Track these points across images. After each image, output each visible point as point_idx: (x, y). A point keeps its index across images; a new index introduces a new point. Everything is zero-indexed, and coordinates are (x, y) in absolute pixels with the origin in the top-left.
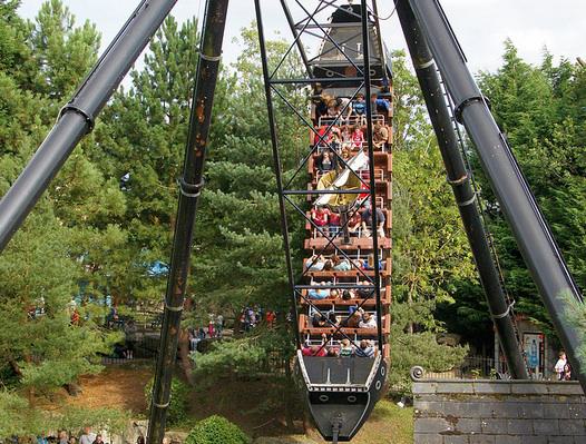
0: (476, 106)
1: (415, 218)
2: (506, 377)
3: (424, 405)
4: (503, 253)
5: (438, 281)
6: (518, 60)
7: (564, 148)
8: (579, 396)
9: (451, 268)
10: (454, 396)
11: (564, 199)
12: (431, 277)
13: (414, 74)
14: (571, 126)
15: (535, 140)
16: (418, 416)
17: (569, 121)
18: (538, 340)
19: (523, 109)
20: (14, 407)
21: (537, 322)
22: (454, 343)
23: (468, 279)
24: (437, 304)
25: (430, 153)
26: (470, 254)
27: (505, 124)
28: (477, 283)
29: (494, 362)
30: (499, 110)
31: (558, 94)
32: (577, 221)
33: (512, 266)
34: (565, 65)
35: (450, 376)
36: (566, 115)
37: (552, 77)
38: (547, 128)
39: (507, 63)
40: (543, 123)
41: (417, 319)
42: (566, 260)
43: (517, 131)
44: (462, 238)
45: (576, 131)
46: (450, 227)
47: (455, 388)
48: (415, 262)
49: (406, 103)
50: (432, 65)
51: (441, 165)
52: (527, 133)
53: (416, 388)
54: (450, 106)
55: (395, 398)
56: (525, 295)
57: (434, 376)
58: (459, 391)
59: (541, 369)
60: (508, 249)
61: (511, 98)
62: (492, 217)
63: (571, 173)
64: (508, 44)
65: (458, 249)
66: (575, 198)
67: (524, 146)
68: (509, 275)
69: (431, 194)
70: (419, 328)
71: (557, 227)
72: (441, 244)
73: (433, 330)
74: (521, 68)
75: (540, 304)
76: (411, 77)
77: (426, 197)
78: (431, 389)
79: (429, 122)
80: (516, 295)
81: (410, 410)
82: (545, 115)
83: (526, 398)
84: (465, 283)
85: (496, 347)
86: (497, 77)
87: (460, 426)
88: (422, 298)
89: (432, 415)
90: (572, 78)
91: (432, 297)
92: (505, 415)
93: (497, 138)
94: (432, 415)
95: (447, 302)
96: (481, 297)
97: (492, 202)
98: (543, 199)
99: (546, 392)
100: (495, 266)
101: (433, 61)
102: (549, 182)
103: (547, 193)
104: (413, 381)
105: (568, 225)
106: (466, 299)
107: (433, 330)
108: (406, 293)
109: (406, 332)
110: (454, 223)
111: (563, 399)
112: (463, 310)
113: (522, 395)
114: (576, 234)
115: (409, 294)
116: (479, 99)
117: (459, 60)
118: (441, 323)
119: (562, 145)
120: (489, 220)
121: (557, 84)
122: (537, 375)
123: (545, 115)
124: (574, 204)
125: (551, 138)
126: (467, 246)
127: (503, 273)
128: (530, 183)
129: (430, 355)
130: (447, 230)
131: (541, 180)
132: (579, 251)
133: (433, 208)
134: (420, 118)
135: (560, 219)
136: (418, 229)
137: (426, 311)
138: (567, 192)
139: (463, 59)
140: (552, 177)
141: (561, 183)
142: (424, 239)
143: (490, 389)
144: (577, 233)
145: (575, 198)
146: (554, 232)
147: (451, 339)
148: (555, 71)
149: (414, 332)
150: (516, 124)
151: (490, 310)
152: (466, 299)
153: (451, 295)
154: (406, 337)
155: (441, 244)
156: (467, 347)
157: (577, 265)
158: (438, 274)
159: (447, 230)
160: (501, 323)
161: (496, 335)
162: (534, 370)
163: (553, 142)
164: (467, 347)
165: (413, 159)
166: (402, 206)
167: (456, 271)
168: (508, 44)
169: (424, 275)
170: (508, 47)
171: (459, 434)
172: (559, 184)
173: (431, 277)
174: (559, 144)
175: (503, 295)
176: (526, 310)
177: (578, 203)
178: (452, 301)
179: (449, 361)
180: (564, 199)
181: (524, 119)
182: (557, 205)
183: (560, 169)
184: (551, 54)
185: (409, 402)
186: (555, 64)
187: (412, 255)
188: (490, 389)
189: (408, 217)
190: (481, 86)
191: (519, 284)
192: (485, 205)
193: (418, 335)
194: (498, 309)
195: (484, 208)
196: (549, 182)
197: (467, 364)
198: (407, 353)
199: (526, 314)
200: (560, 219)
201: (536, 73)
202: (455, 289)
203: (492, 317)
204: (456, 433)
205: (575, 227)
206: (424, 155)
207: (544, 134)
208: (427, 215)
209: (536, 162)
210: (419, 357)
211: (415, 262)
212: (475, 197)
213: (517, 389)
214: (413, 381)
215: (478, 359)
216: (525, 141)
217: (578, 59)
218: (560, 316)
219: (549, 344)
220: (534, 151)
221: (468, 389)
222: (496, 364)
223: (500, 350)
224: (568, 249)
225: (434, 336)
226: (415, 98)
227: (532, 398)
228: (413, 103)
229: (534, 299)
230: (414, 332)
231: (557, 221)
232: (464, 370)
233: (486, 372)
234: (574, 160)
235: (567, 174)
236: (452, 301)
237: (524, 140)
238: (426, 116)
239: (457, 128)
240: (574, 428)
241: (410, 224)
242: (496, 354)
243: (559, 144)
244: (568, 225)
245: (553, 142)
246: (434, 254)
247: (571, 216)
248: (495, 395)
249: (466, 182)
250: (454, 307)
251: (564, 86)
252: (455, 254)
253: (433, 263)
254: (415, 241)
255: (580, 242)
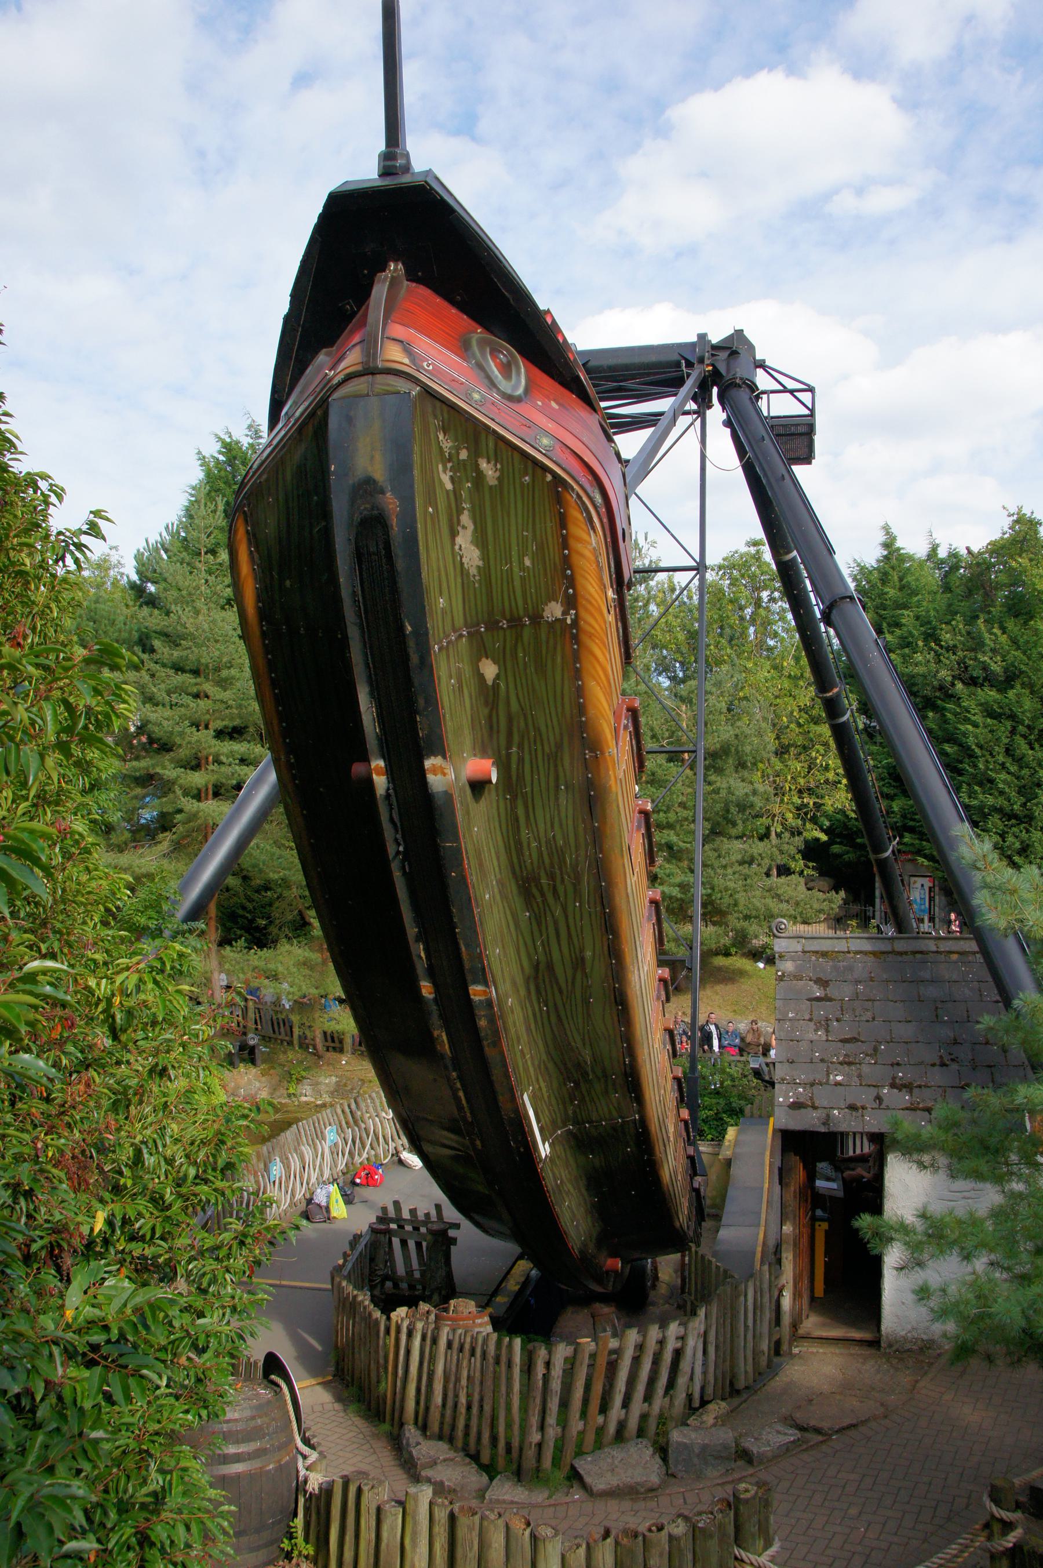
0: (847, 605)
1: (778, 738)
2: (890, 931)
3: (788, 966)
4: (883, 779)
5: (806, 814)
6: (899, 549)
7: (954, 654)
8: (974, 953)
9: (822, 797)
10: (824, 954)
11: (956, 714)
12: (798, 809)
13: (774, 567)
14: (961, 626)
15: (920, 643)
16: (781, 979)
17: (959, 622)
18: (927, 883)
19: (905, 607)
20: (306, 963)
21: (926, 863)
22: (826, 888)
23: (842, 812)
24: (806, 842)
25: (797, 659)
26: (844, 781)
27: (885, 625)
28: (853, 815)
29: (874, 911)
30: (877, 608)
31: (947, 588)
32: (971, 741)
33: (895, 795)
34: (954, 555)
35: (820, 929)
36: (956, 613)
37: (939, 569)
38: (934, 628)
39: (885, 553)
40: (929, 623)
41: (780, 860)
42: (958, 790)
43: (898, 632)
44: (834, 761)
45: (969, 633)
46: (821, 749)
47: (825, 946)
48: (779, 791)
49: (766, 600)
50: (795, 558)
51: (808, 673)
52: (910, 633)
53: (779, 946)
54: (817, 605)
55: (756, 955)
56: (911, 830)
57: (802, 928)
58: (830, 949)
59: (932, 919)
60: (889, 774)
61: (891, 592)
62: (871, 736)
63: (964, 683)
64: (887, 529)
65: (831, 775)
66: (969, 712)
67: (907, 651)
68: (891, 807)
69: (797, 709)
70: (784, 871)
71: (948, 748)
72: (810, 768)
73: (801, 873)
74: (902, 558)
75: (928, 841)
76: (772, 570)
77: (792, 712)
78: (796, 946)
79: (793, 623)
80: (900, 830)
81: (771, 970)
82: (932, 613)
83: (910, 957)
84: (839, 816)
85: (877, 893)
86: (875, 569)
87: (832, 991)
88: (787, 835)
89: (798, 977)
90: (962, 571)
91: (800, 833)
92: (885, 976)
93: (873, 646)
94: (798, 977)
95: (817, 840)
96: (858, 833)
97: (869, 717)
98: (931, 714)
99: (934, 949)
100: (873, 796)
101: (795, 553)
102: (938, 694)
103: (935, 708)
104: (775, 936)
105: (960, 745)
106: (840, 835)
107: (801, 873)
108: (768, 828)
109: (768, 875)
110: (826, 744)
111: (955, 957)
112: (836, 849)
113: (906, 953)
114: (971, 756)
115: (772, 829)
116: (851, 598)
117: (825, 552)
118: (811, 864)
119: (952, 649)
120: (867, 739)
121: (945, 576)
122: (926, 926)
123: (932, 613)
124: (967, 720)
125: (937, 641)
126: (841, 771)
127: (883, 804)
128: (912, 693)
129: (797, 904)
130: (818, 751)
131: (927, 692)
132: (974, 776)
133: (799, 725)
134: (782, 619)
135: (951, 739)
136: (782, 752)
137: (793, 850)
138: (960, 706)
139: (830, 551)
140: (941, 688)
141: (952, 696)
142: (789, 763)
143: (867, 946)
144: (972, 756)
145: (969, 712)
146: (942, 754)
147: (824, 883)
148: (942, 562)
149: (779, 875)
150: (898, 625)
151: (869, 849)
152: (840, 835)
153: (822, 830)
154: (768, 882)
155: (810, 768)
156: (842, 894)
157: (971, 794)
158: (806, 805)
159: (818, 751)
160: (883, 864)
161: (877, 878)
162: (922, 921)
163: (941, 647)
164: (842, 894)
165: (775, 667)
166: (764, 725)
167: (828, 801)
168: (887, 529)
169: (790, 807)
170: (888, 533)
171: (830, 1000)
172: (950, 697)
173: (798, 809)
174: (948, 649)
175: (884, 830)
176: (913, 850)
177: (973, 718)
178: (824, 837)
179: (820, 911)
180: (956, 714)
181: (907, 617)
182: (946, 721)
183: (949, 679)
184: (937, 542)
185: (770, 961)
186: (942, 553)
187: (774, 782)
188: (867, 946)
189: (770, 737)
190: (855, 579)
191: (904, 816)
192: (861, 722)
193: (783, 879)
194: (879, 848)
195: (861, 726)
196: (938, 694)
197: (842, 914)
198: (769, 901)
199: (912, 853)
200: (951, 739)
201: (921, 564)
202: (827, 823)
203: (872, 857)
204: (826, 999)
205: (969, 748)
206: (788, 663)
207: (931, 636)
208: (794, 734)
209: (921, 670)
210: (784, 906)
211: (779, 791)
212: (849, 713)
213: (900, 946)
214: (775, 936)
215: (855, 908)
216: (908, 645)
217: (968, 548)
218: (952, 857)
219: (940, 889)
220: (919, 657)
221: (841, 946)
222: (877, 914)
223: (882, 897)
224: (961, 775)
225: (802, 880)
226: (776, 594)
227: (918, 956)
228: (772, 600)
229: (922, 836)
230: (779, 875)
231: (948, 741)
232: (838, 922)
233: (865, 921)
234: (966, 668)
235: (959, 686)
236: (824, 837)
237: (906, 643)
238: (790, 616)
239: (826, 632)
240: (967, 991)
241: (772, 745)
242: (878, 901)
243: (948, 649)
244: (960, 745)
245: (941, 647)
246: (802, 781)
247: (964, 734)
248: (874, 953)
249: (838, 695)
250: (827, 845)
251: (954, 581)
252: (827, 781)
253: (800, 792)
254: (779, 766)
255: (975, 766)
